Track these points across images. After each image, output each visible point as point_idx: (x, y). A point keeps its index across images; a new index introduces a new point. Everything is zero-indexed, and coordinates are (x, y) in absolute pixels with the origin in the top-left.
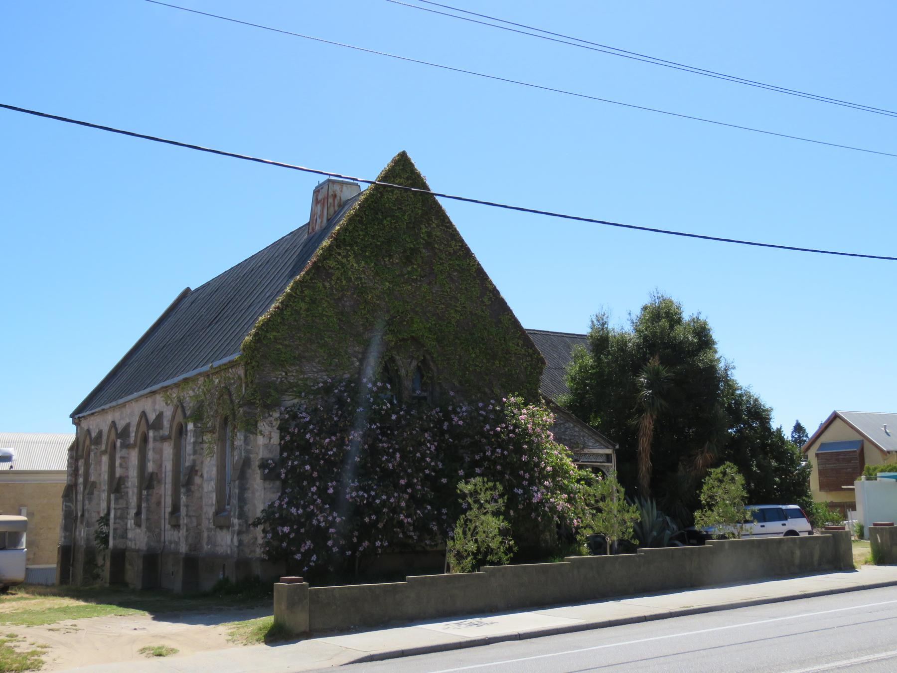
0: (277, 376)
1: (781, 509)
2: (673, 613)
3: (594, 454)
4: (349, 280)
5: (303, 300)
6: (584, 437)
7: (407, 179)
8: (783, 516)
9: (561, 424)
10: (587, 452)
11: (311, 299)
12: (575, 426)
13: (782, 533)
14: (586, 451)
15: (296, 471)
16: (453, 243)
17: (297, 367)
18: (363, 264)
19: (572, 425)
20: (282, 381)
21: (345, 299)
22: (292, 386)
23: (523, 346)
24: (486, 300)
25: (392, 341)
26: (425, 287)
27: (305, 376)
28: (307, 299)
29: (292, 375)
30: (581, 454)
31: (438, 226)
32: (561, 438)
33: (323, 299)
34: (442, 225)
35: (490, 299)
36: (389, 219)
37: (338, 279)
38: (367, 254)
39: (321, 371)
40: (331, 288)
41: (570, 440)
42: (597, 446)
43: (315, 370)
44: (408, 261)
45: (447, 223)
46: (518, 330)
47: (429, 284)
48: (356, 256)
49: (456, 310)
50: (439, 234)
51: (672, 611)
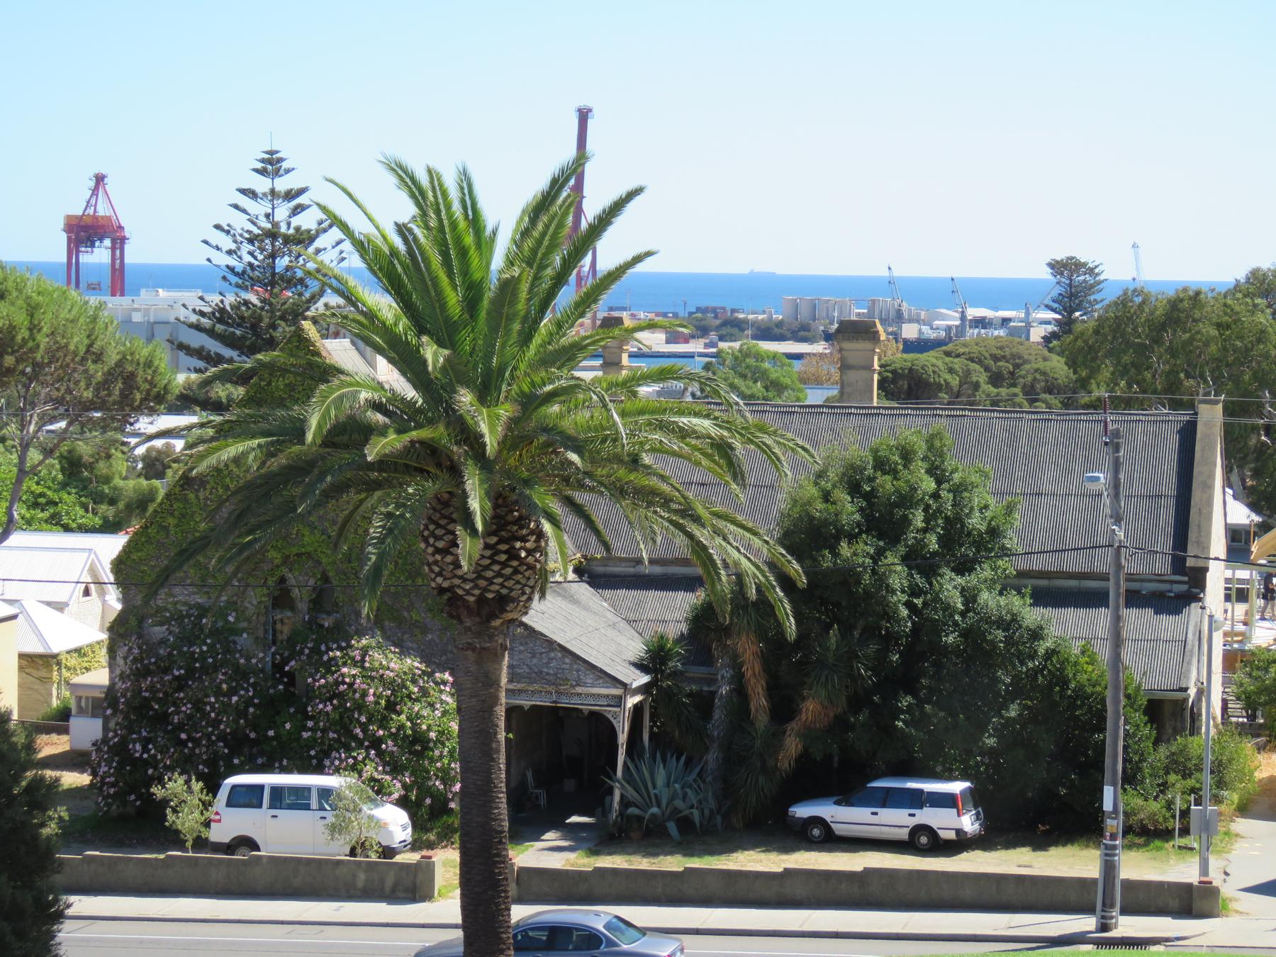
1: (921, 791)
5: (172, 515)
8: (917, 800)
9: (541, 653)
12: (564, 656)
14: (579, 690)
19: (559, 655)
28: (176, 513)
32: (541, 672)
39: (194, 593)
40: (206, 499)
41: (556, 674)
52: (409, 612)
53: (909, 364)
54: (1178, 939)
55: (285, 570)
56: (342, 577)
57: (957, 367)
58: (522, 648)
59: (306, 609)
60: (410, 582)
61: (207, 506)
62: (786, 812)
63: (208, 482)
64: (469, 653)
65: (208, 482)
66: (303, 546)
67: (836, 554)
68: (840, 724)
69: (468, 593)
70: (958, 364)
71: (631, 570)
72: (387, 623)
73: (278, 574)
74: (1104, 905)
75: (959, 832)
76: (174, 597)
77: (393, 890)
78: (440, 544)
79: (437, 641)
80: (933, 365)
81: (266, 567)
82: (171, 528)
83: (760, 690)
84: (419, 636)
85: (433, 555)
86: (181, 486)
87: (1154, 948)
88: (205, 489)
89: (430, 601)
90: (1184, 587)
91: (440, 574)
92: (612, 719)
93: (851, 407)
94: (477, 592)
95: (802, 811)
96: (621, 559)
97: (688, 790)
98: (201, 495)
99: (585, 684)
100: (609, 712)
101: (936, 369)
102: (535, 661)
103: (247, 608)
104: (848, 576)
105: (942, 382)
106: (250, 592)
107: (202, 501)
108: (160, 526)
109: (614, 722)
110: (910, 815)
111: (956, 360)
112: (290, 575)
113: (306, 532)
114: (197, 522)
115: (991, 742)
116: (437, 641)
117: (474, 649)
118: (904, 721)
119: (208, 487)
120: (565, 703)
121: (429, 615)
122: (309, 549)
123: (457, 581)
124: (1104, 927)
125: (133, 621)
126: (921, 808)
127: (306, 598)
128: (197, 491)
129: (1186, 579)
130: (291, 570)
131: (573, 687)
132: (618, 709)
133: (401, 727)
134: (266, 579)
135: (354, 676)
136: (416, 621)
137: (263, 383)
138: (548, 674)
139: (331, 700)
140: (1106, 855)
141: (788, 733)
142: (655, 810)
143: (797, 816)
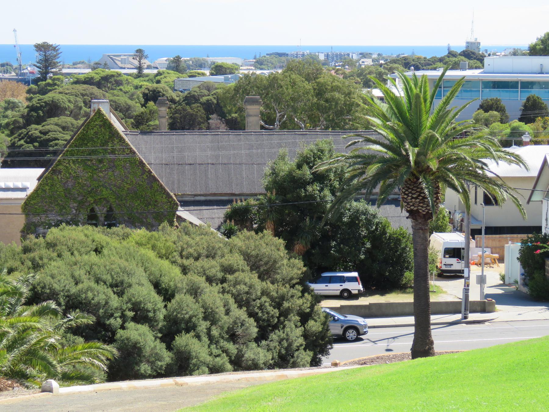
0: (35, 219)
1: (344, 276)
4: (70, 174)
5: (47, 185)
7: (101, 121)
8: (342, 280)
18: (77, 165)
20: (38, 221)
22: (42, 223)
23: (166, 198)
24: (145, 176)
26: (110, 173)
28: (49, 184)
31: (118, 142)
34: (120, 142)
35: (147, 176)
36: (91, 143)
40: (62, 178)
47: (113, 171)
49: (127, 183)
52: (146, 219)
53: (51, 99)
54: (492, 320)
55: (94, 205)
57: (72, 99)
60: (146, 207)
61: (61, 181)
63: (62, 172)
64: (421, 231)
65: (62, 172)
66: (103, 195)
67: (306, 190)
69: (424, 211)
70: (72, 98)
71: (192, 199)
72: (137, 224)
73: (91, 207)
74: (465, 310)
75: (359, 290)
78: (415, 196)
80: (62, 99)
81: (87, 204)
82: (47, 190)
85: (411, 199)
86: (52, 173)
87: (487, 323)
88: (61, 174)
89: (154, 215)
91: (413, 205)
93: (251, 132)
94: (426, 211)
96: (189, 195)
98: (59, 177)
101: (63, 101)
104: (312, 197)
105: (67, 107)
107: (60, 179)
108: (42, 190)
110: (341, 285)
111: (71, 97)
112: (96, 207)
113: (104, 190)
114: (57, 188)
115: (363, 257)
117: (422, 230)
118: (334, 251)
121: (154, 220)
122: (105, 196)
123: (420, 208)
124: (466, 318)
126: (344, 283)
127: (103, 215)
128: (58, 175)
137: (85, 132)
140: (466, 292)
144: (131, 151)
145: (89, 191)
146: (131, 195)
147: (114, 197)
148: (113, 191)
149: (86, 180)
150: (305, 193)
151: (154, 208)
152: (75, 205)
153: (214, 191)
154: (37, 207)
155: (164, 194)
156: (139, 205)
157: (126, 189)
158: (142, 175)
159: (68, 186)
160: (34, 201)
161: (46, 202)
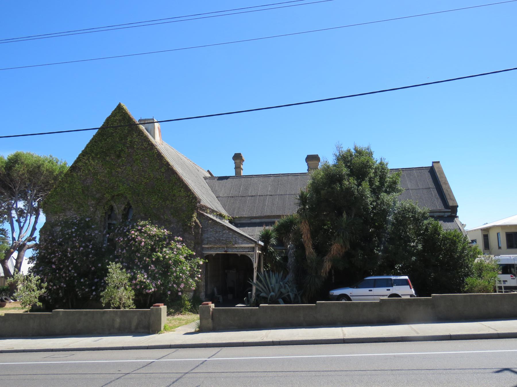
2: (274, 341)
3: (242, 247)
4: (89, 170)
5: (67, 183)
6: (235, 238)
8: (389, 284)
9: (220, 231)
10: (236, 246)
11: (70, 182)
12: (229, 232)
13: (387, 295)
14: (236, 246)
15: (65, 261)
16: (145, 143)
17: (64, 214)
18: (96, 161)
19: (227, 232)
21: (88, 180)
23: (184, 191)
25: (109, 197)
27: (67, 217)
28: (69, 182)
29: (61, 218)
30: (233, 248)
31: (137, 136)
33: (76, 181)
34: (139, 136)
37: (83, 171)
38: (98, 156)
39: (75, 214)
42: (245, 243)
43: (71, 214)
44: (119, 156)
45: (142, 134)
46: (181, 184)
47: (131, 166)
48: (93, 159)
50: (137, 140)
51: (452, 334)
52: (163, 215)
56: (135, 203)
58: (211, 230)
59: (121, 218)
60: (164, 203)
62: (329, 293)
63: (82, 169)
65: (82, 169)
68: (348, 256)
71: (249, 221)
72: (154, 221)
76: (67, 216)
77: (136, 328)
79: (175, 226)
82: (66, 188)
83: (310, 246)
84: (168, 226)
88: (80, 171)
89: (172, 210)
90: (450, 213)
92: (250, 257)
95: (337, 292)
96: (245, 217)
97: (286, 285)
99: (239, 243)
100: (249, 254)
102: (217, 235)
103: (96, 218)
104: (348, 191)
106: (98, 212)
107: (79, 177)
109: (252, 259)
110: (387, 290)
116: (175, 226)
119: (82, 170)
120: (230, 252)
121: (172, 216)
122: (122, 192)
125: (49, 227)
126: (392, 286)
128: (77, 172)
129: (450, 210)
130: (115, 202)
131: (234, 245)
132: (253, 253)
133: (158, 257)
134: (105, 206)
135: (136, 235)
136: (166, 219)
138: (222, 240)
139: (125, 248)
141: (325, 261)
142: (272, 293)
143: (334, 294)
144: (149, 144)
145: (106, 188)
146: (148, 190)
147: (130, 192)
148: (130, 187)
149: (104, 177)
150: (341, 187)
151: (172, 203)
152: (92, 202)
153: (268, 214)
154: (55, 205)
155: (182, 187)
156: (157, 200)
157: (143, 183)
158: (160, 168)
159: (87, 183)
160: (53, 199)
161: (64, 200)
